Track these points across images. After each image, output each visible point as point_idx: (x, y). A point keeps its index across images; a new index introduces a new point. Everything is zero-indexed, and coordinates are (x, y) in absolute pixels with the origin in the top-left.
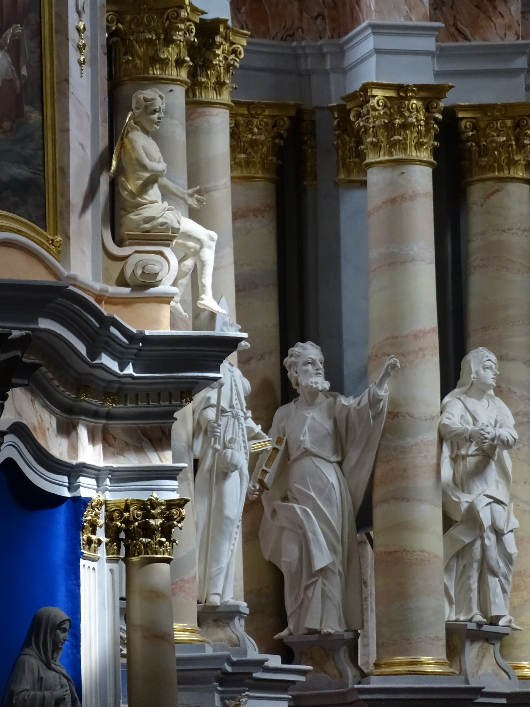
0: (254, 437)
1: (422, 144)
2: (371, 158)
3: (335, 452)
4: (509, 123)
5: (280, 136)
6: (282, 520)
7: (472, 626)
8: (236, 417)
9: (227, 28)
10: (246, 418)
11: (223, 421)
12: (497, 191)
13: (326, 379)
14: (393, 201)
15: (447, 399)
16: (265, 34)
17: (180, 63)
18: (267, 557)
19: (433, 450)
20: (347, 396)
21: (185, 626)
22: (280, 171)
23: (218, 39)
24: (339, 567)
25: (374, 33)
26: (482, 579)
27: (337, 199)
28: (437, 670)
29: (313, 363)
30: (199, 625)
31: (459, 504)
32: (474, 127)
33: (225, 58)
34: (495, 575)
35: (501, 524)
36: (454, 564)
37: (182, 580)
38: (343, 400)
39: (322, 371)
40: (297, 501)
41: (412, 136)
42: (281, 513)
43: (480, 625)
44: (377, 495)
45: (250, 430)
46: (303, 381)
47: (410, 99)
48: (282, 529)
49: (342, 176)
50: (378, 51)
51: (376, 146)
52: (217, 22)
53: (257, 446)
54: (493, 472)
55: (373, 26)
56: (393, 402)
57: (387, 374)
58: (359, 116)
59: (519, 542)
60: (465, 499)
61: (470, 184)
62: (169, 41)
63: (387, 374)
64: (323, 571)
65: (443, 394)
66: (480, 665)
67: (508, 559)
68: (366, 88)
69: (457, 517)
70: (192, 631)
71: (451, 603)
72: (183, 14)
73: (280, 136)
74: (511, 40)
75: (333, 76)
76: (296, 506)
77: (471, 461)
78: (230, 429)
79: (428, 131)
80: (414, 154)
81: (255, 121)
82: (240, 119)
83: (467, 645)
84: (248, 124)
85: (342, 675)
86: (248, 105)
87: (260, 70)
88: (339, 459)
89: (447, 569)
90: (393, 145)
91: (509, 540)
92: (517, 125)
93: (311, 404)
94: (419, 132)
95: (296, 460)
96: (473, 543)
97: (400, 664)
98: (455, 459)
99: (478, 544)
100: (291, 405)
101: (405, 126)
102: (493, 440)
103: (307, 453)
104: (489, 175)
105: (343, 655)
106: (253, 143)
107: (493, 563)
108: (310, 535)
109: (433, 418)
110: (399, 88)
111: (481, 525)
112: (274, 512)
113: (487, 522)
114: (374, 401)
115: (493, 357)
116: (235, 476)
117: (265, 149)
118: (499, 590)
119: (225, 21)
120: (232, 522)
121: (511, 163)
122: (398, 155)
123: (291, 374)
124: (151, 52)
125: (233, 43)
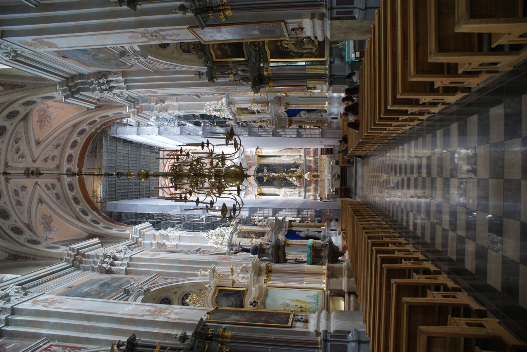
60: (289, 195)
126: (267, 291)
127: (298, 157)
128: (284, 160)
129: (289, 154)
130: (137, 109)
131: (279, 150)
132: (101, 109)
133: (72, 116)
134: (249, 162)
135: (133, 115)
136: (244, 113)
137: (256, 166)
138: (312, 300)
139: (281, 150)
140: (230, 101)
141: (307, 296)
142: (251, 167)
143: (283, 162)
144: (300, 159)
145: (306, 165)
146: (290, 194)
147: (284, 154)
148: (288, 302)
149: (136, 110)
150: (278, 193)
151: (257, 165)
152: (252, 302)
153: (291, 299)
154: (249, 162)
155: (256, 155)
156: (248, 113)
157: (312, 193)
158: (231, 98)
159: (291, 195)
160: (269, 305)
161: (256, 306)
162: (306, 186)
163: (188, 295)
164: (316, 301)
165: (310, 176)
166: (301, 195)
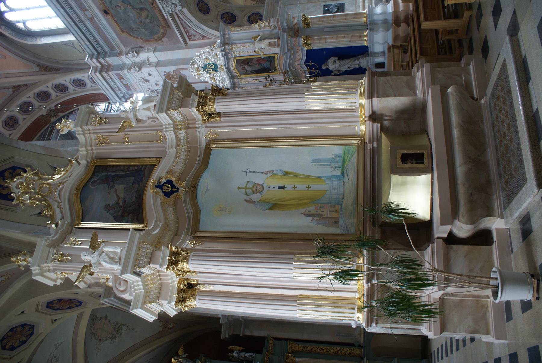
126: (208, 150)
130: (103, 66)
132: (58, 72)
133: (15, 71)
135: (93, 71)
136: (246, 73)
138: (328, 171)
140: (226, 41)
141: (314, 161)
148: (259, 180)
149: (99, 65)
152: (164, 180)
153: (268, 172)
156: (253, 72)
158: (227, 36)
160: (208, 190)
161: (171, 196)
163: (18, 171)
164: (339, 173)
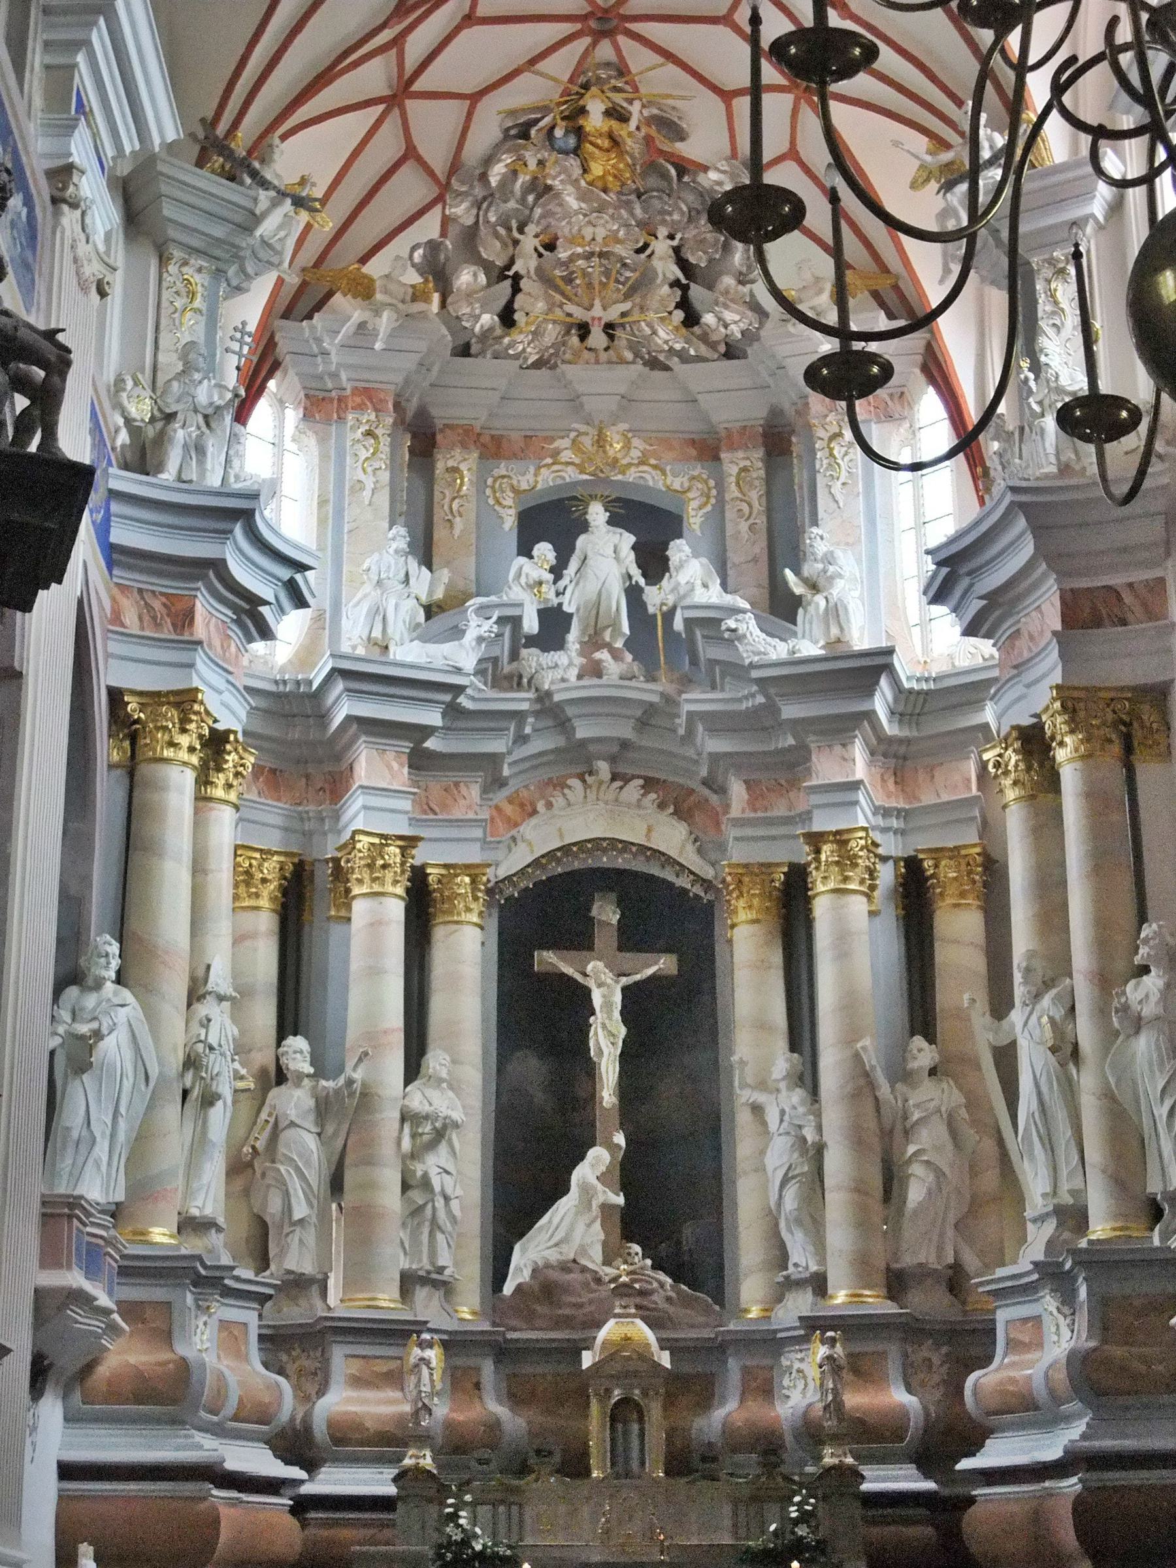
0: (239, 1077)
1: (398, 882)
2: (356, 891)
3: (317, 1124)
4: (467, 880)
5: (285, 878)
6: (269, 1180)
7: (421, 1273)
8: (223, 1054)
9: (237, 741)
10: (233, 1060)
11: (212, 1057)
12: (456, 931)
13: (312, 1064)
14: (372, 924)
15: (409, 1088)
16: (279, 800)
17: (192, 749)
18: (255, 1211)
19: (397, 1125)
20: (328, 1080)
21: (165, 1231)
22: (284, 906)
23: (228, 747)
24: (314, 1219)
25: (363, 793)
26: (432, 1234)
27: (327, 932)
28: (392, 1306)
29: (301, 1052)
30: (179, 1232)
31: (415, 1171)
32: (439, 882)
33: (235, 767)
34: (443, 1232)
35: (449, 1191)
36: (409, 1220)
37: (166, 1190)
38: (323, 1083)
39: (308, 1059)
40: (282, 1163)
41: (389, 875)
42: (270, 1174)
43: (429, 1272)
44: (348, 1161)
45: (236, 1071)
46: (292, 1066)
47: (387, 845)
48: (269, 1186)
49: (333, 913)
50: (365, 807)
51: (360, 881)
52: (228, 732)
53: (241, 1085)
54: (443, 1148)
55: (361, 787)
56: (364, 1085)
57: (360, 1060)
58: (348, 861)
59: (462, 1209)
60: (419, 1169)
61: (434, 925)
62: (184, 731)
63: (360, 1060)
64: (301, 1221)
65: (406, 1085)
66: (426, 1307)
67: (453, 1219)
68: (355, 832)
69: (412, 1182)
70: (171, 1236)
71: (405, 1253)
72: (196, 707)
73: (285, 878)
74: (471, 816)
75: (330, 836)
76: (282, 1168)
77: (426, 1138)
78: (217, 1065)
79: (403, 872)
80: (390, 889)
81: (266, 865)
82: (254, 862)
83: (418, 1287)
84: (260, 865)
85: (312, 1307)
86: (261, 851)
87: (273, 826)
88: (318, 1130)
89: (404, 1225)
90: (374, 880)
91: (455, 1205)
92: (473, 882)
93: (298, 1085)
94: (395, 872)
95: (284, 1129)
96: (425, 1204)
97: (360, 1300)
98: (414, 1136)
99: (430, 1206)
100: (283, 1087)
101: (384, 867)
102: (445, 1118)
103: (293, 1124)
104: (450, 919)
105: (315, 1290)
106: (264, 881)
107: (441, 1222)
108: (291, 1191)
109: (396, 1099)
110: (381, 836)
111: (432, 1191)
112: (263, 1175)
113: (437, 1189)
114: (350, 1082)
115: (448, 1058)
116: (220, 1104)
117: (272, 887)
118: (445, 1245)
119: (235, 733)
120: (214, 1145)
121: (468, 910)
122: (376, 888)
123: (283, 1060)
124: (166, 737)
125: (242, 758)
127: (801, 1258)
128: (772, 1117)
129: (837, 1163)
131: (873, 1059)
134: (737, 790)
137: (690, 858)
139: (872, 1085)
142: (680, 813)
143: (744, 1117)
144: (790, 1284)
145: (719, 1348)
146: (426, 1183)
147: (834, 1116)
150: (436, 1061)
151: (708, 873)
154: (737, 790)
155: (815, 840)
157: (442, 1410)
159: (418, 1197)
162: (503, 1352)
165: (626, 1376)
166: (421, 1294)
